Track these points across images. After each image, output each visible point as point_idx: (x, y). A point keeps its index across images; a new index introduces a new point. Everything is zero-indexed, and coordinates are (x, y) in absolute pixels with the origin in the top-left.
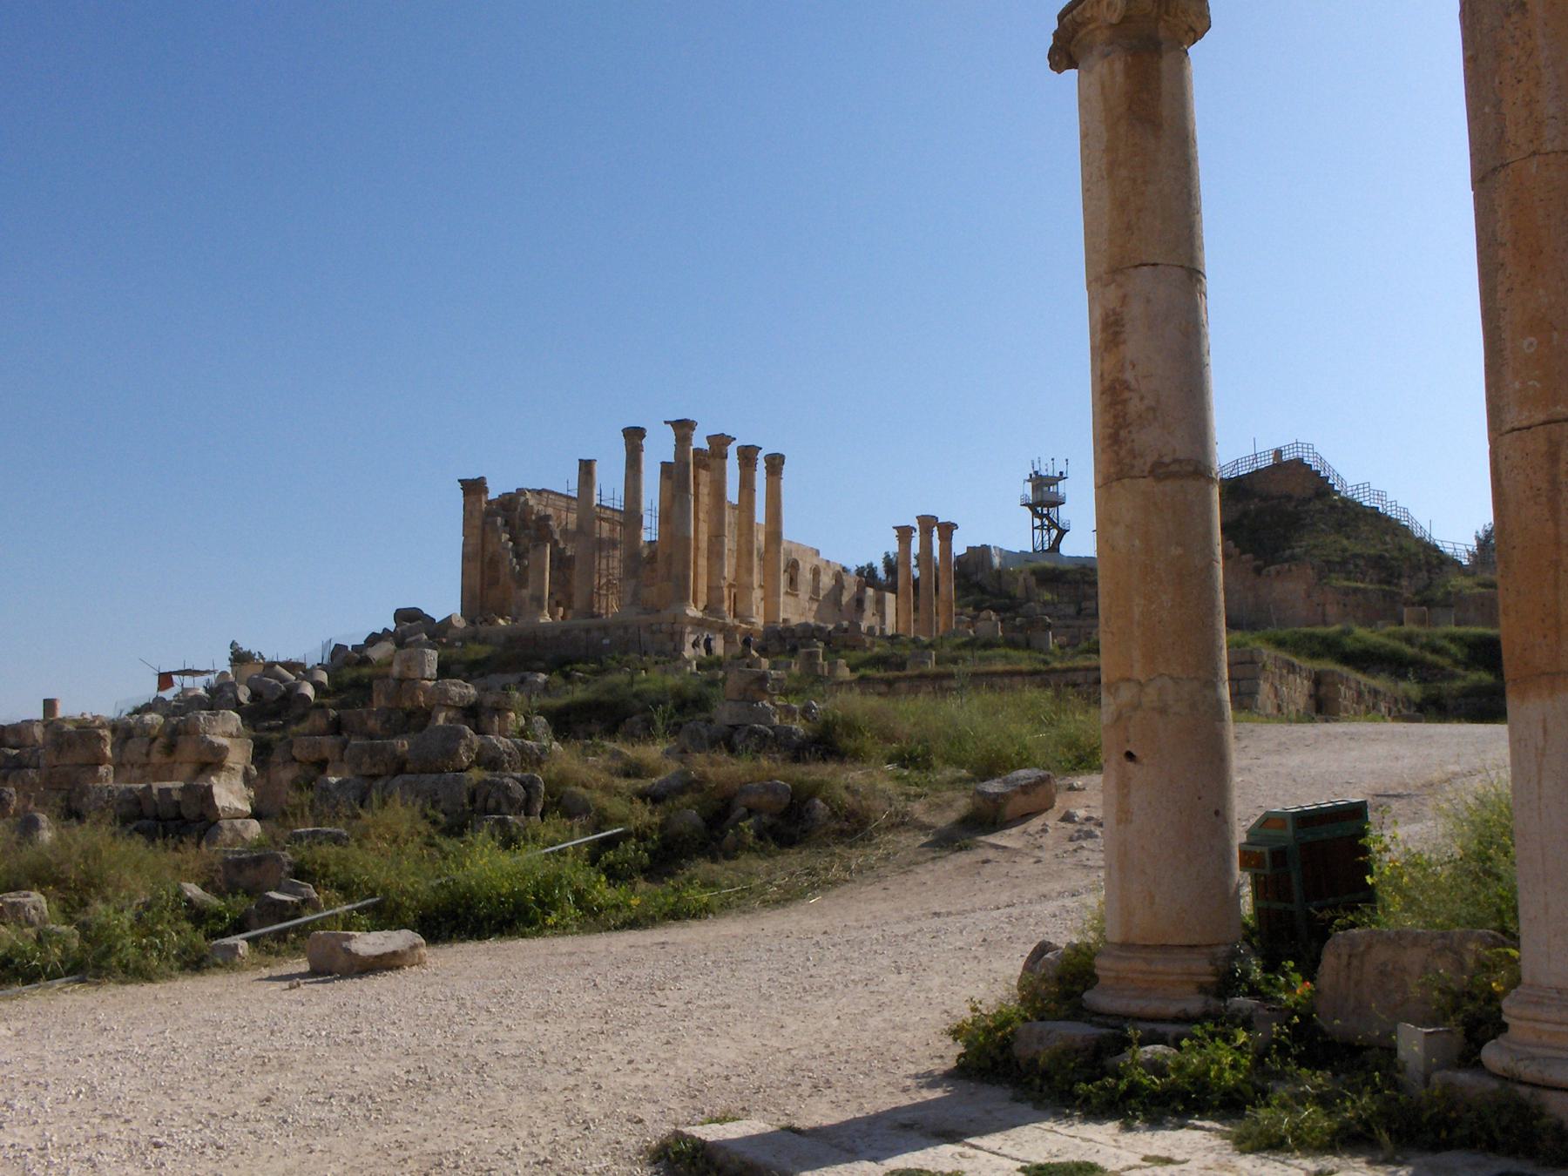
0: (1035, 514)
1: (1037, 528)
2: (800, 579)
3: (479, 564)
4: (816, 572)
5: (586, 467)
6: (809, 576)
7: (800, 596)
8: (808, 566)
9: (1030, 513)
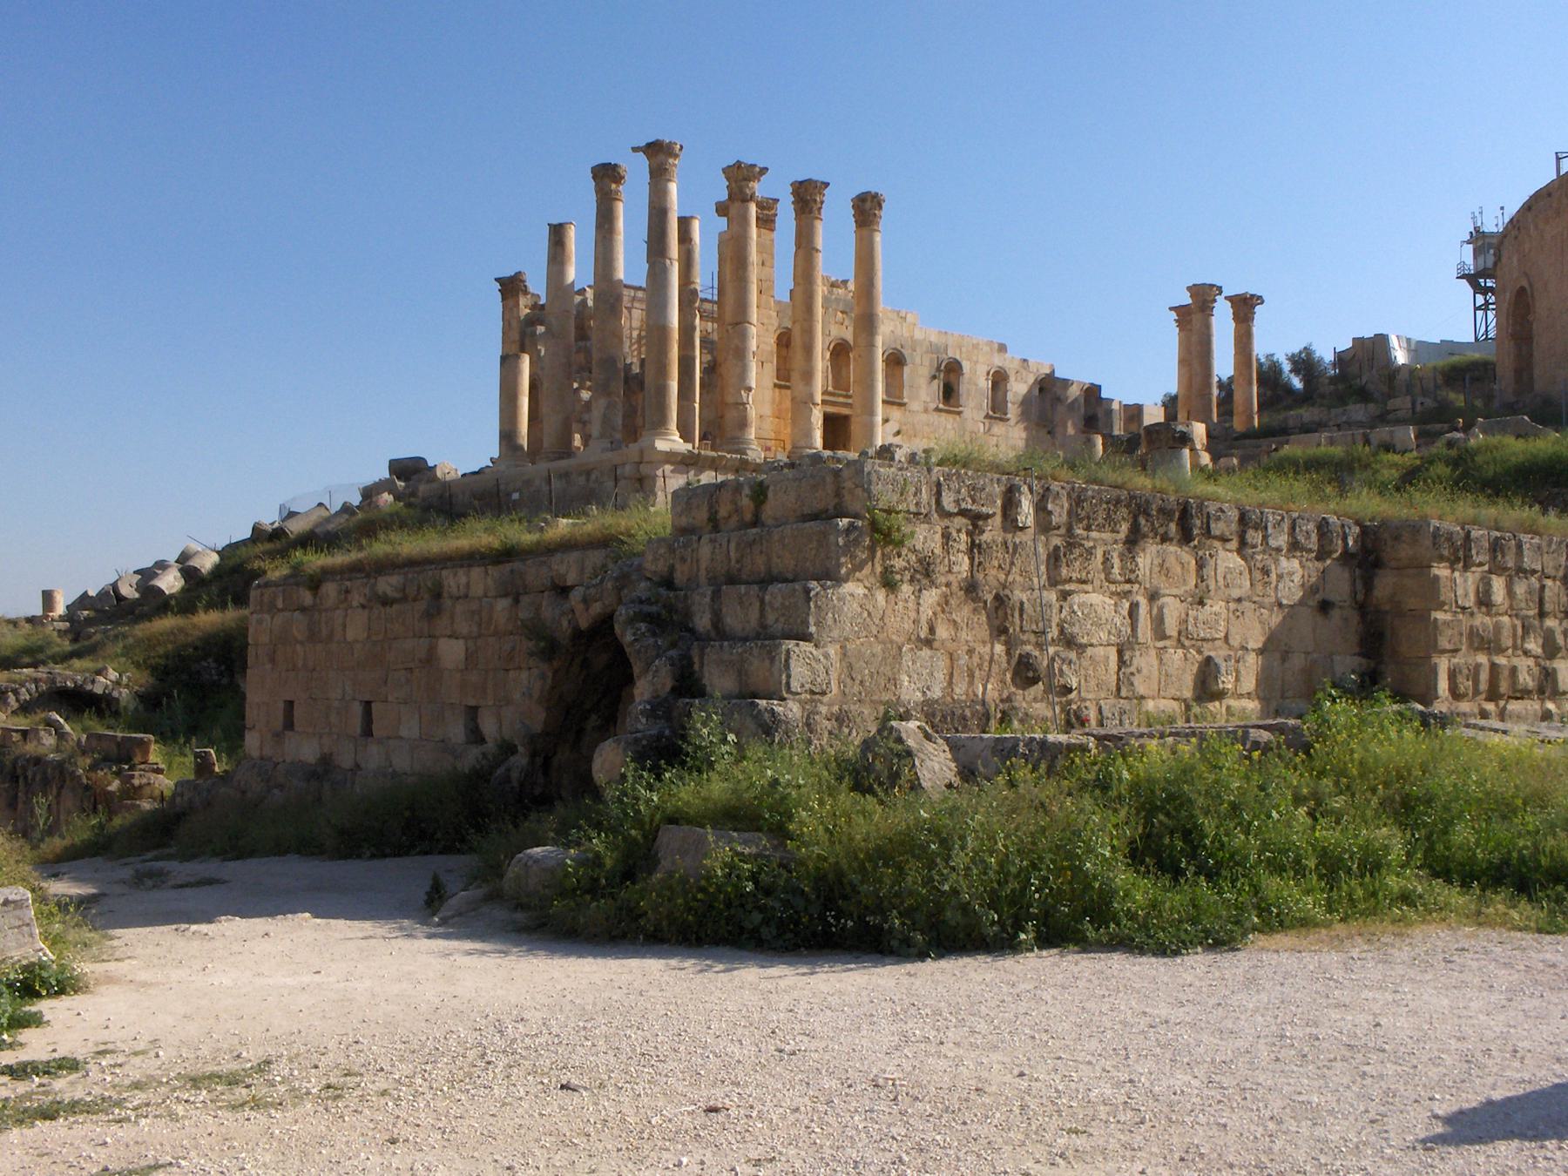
0: (1478, 289)
1: (1479, 308)
2: (964, 388)
4: (999, 380)
5: (557, 234)
6: (985, 384)
8: (982, 370)
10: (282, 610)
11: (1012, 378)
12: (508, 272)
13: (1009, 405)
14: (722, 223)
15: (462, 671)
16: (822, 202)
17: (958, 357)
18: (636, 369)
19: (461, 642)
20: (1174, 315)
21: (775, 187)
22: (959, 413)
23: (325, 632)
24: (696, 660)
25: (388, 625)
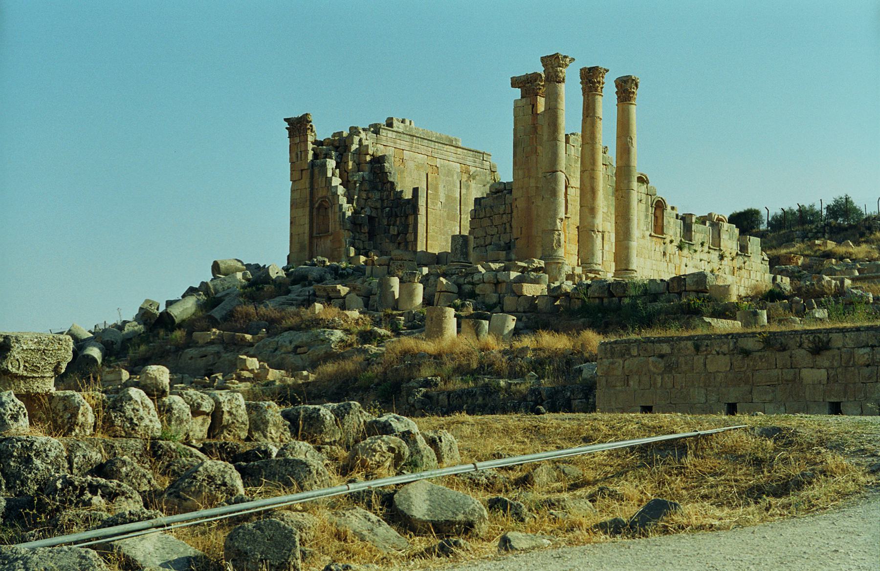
3: (308, 209)
10: (635, 356)
12: (297, 114)
14: (517, 93)
18: (408, 195)
19: (823, 371)
23: (684, 367)
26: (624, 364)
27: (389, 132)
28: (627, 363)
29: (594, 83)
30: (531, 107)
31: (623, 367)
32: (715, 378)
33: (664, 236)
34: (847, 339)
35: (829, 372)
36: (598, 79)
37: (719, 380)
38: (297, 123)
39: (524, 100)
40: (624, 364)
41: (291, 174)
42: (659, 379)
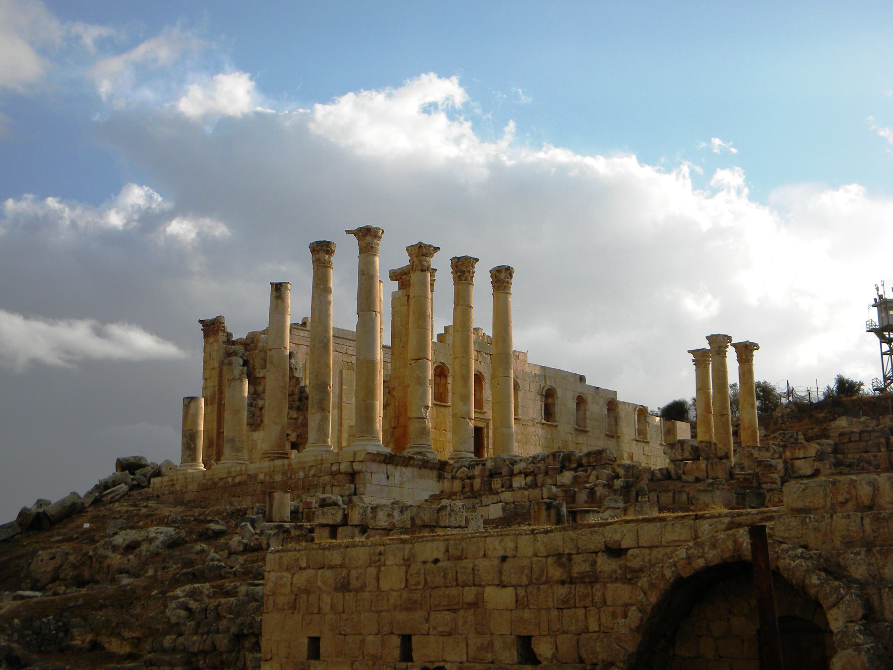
0: (883, 339)
1: (885, 353)
2: (558, 409)
3: (216, 405)
5: (278, 289)
7: (559, 428)
9: (877, 340)
10: (305, 569)
11: (589, 401)
12: (210, 316)
13: (588, 421)
14: (395, 285)
15: (511, 610)
16: (474, 272)
17: (553, 385)
19: (510, 590)
20: (691, 357)
21: (441, 263)
22: (556, 426)
24: (875, 598)
25: (429, 578)
26: (292, 579)
27: (301, 331)
28: (296, 576)
29: (463, 272)
30: (406, 297)
31: (292, 584)
32: (388, 600)
33: (556, 423)
34: (539, 544)
35: (518, 593)
36: (468, 269)
37: (392, 601)
38: (212, 325)
39: (401, 291)
40: (292, 579)
41: (204, 373)
42: (326, 598)
